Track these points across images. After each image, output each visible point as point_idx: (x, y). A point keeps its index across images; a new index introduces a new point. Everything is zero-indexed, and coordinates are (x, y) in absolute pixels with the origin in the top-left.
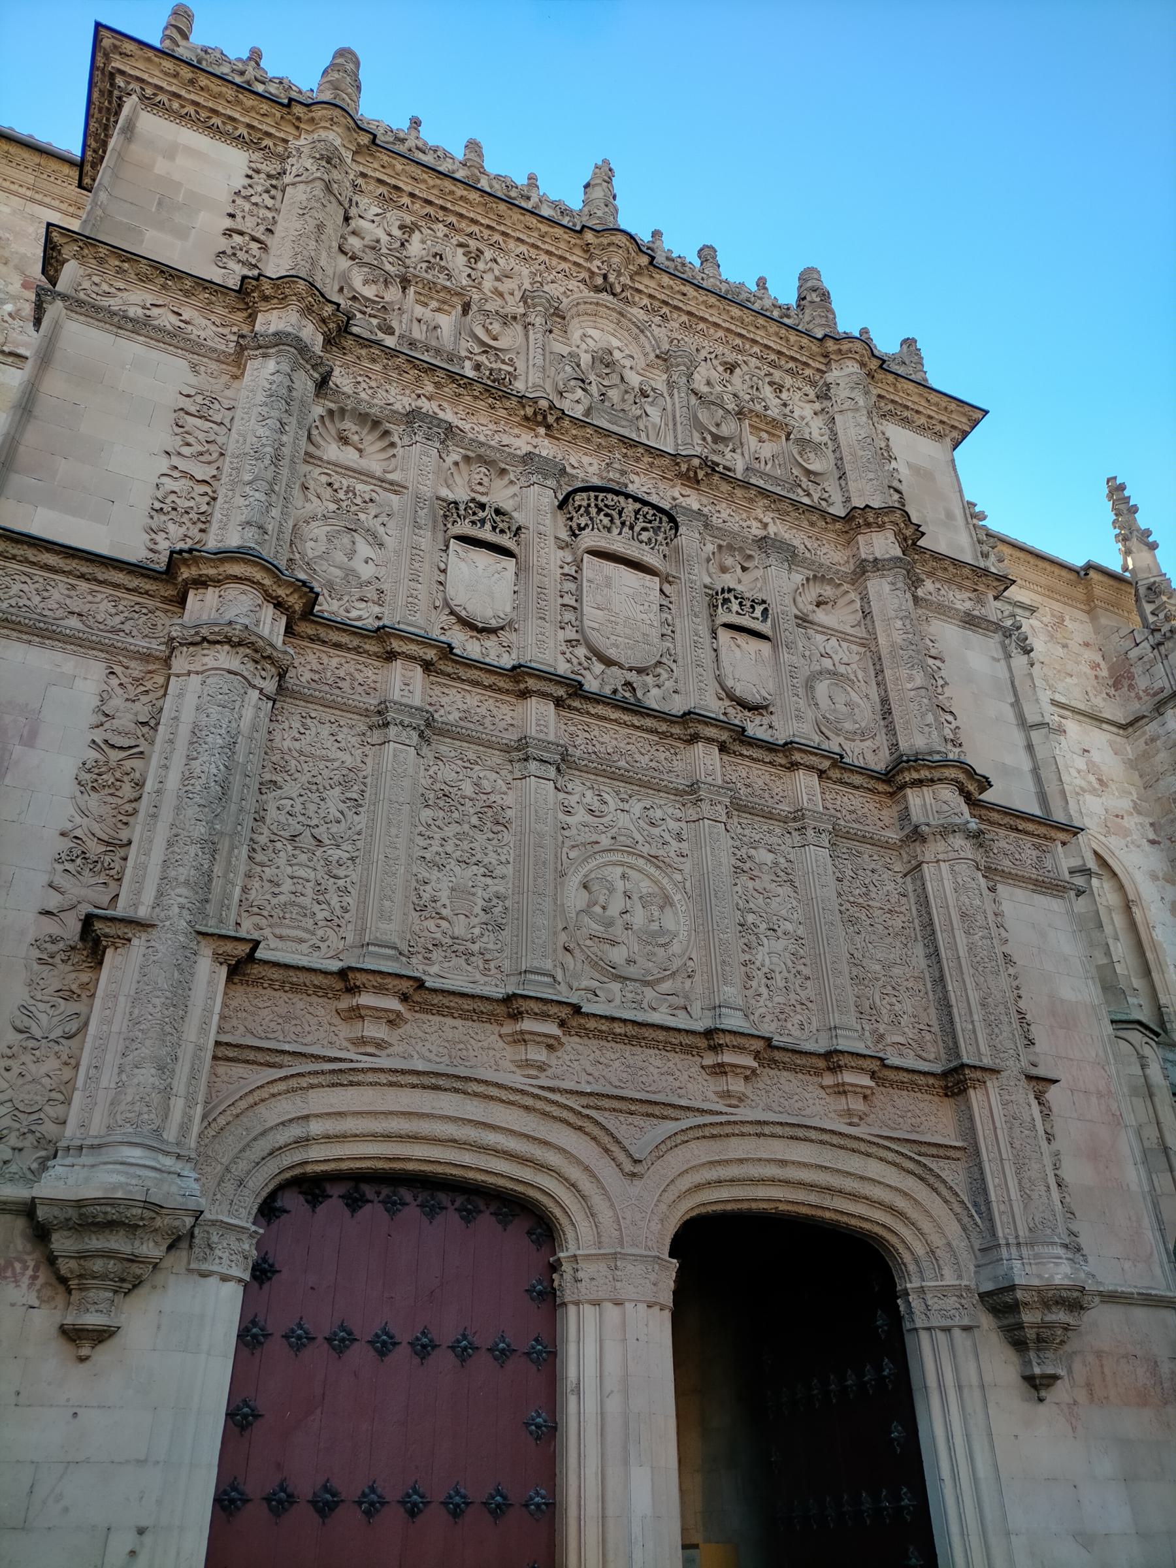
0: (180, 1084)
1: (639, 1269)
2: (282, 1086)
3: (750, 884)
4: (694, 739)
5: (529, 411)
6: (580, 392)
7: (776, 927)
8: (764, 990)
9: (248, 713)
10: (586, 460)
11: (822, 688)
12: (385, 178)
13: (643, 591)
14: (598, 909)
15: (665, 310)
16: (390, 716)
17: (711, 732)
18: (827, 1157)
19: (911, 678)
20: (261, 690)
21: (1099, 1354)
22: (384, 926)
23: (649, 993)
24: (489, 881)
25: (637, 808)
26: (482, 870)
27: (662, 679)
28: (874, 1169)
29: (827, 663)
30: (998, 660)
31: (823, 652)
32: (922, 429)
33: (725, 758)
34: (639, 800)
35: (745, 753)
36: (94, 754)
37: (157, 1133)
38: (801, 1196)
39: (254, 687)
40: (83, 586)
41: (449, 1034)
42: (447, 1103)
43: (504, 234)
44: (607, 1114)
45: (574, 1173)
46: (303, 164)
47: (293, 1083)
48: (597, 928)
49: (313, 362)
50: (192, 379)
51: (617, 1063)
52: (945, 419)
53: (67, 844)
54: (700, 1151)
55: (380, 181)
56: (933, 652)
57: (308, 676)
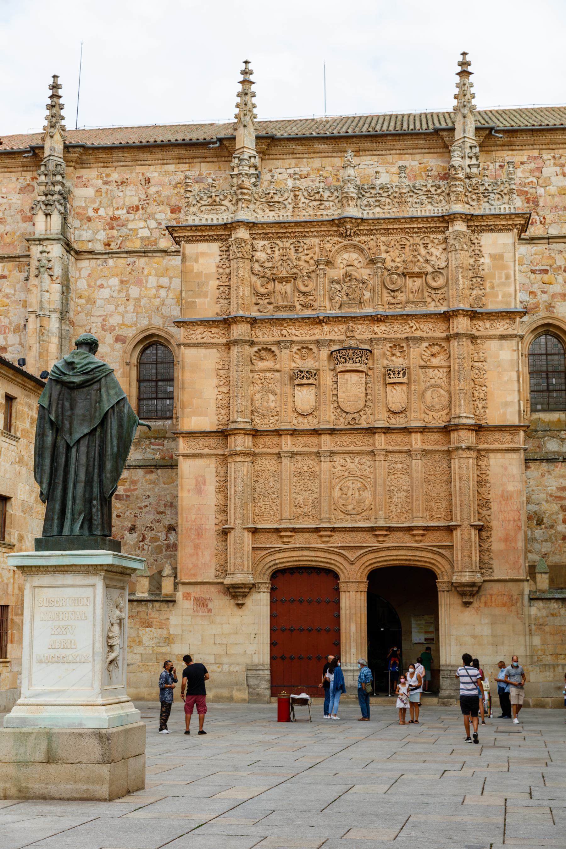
0: (246, 560)
1: (354, 584)
3: (393, 477)
4: (374, 433)
5: (318, 321)
6: (337, 298)
8: (394, 510)
9: (246, 469)
10: (340, 327)
11: (429, 393)
12: (262, 231)
15: (375, 231)
16: (282, 455)
17: (379, 430)
18: (409, 553)
19: (459, 386)
21: (491, 595)
22: (286, 514)
23: (359, 517)
25: (357, 460)
28: (424, 554)
29: (433, 381)
30: (515, 351)
31: (431, 376)
32: (500, 230)
36: (218, 484)
37: (243, 570)
38: (403, 562)
40: (206, 438)
41: (305, 537)
42: (306, 553)
43: (307, 232)
45: (338, 564)
46: (234, 248)
48: (342, 502)
50: (218, 355)
52: (511, 222)
53: (216, 508)
55: (260, 234)
56: (482, 359)
57: (261, 446)
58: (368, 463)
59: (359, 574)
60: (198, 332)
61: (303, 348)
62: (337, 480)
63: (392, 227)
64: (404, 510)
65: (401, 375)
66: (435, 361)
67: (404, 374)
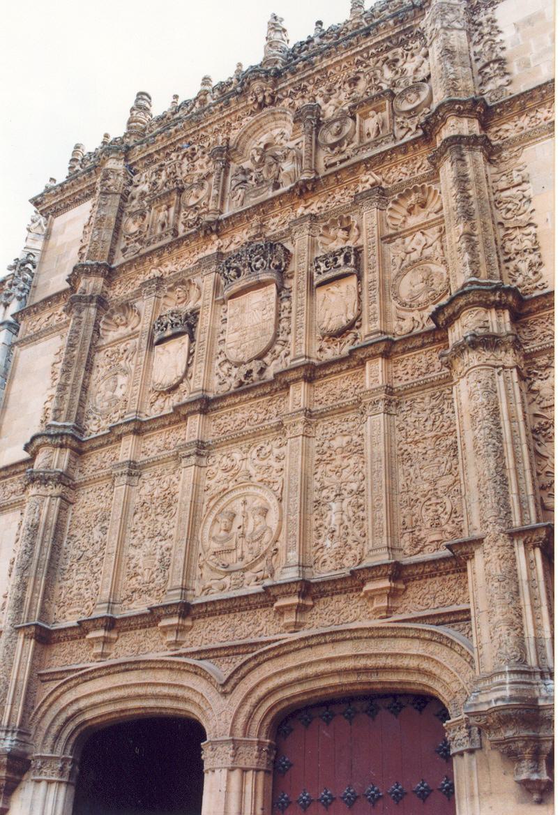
2: (65, 688)
6: (240, 191)
7: (343, 492)
8: (328, 543)
9: (44, 511)
13: (265, 299)
14: (223, 533)
17: (294, 375)
18: (364, 647)
20: (51, 496)
23: (248, 575)
24: (163, 543)
26: (160, 538)
27: (277, 352)
28: (400, 646)
31: (409, 249)
33: (316, 384)
34: (255, 447)
35: (328, 372)
38: (352, 679)
39: (47, 496)
42: (132, 678)
44: (212, 660)
47: (68, 685)
49: (88, 300)
51: (223, 627)
54: (268, 669)
55: (142, 159)
58: (276, 451)
59: (241, 720)
60: (43, 320)
61: (176, 284)
62: (212, 504)
63: (330, 63)
64: (350, 539)
65: (341, 261)
66: (413, 221)
67: (347, 259)
